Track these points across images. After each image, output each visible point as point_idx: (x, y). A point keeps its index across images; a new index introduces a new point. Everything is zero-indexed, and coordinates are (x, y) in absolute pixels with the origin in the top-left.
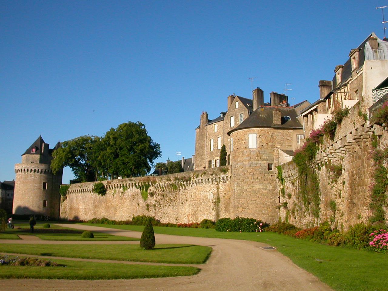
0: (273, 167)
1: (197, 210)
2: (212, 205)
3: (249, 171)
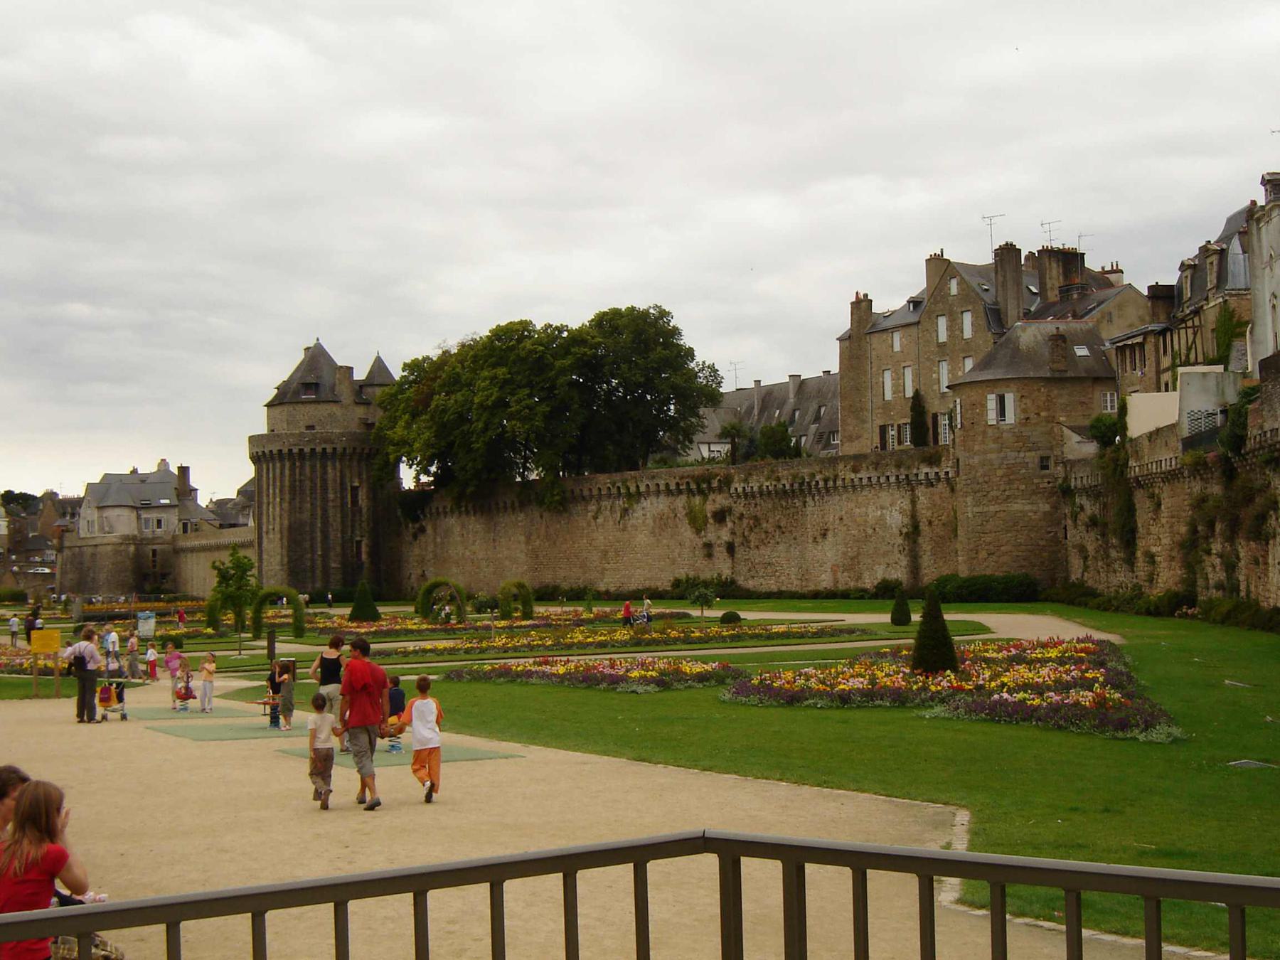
0: (1051, 463)
1: (859, 554)
2: (900, 540)
3: (1000, 473)
